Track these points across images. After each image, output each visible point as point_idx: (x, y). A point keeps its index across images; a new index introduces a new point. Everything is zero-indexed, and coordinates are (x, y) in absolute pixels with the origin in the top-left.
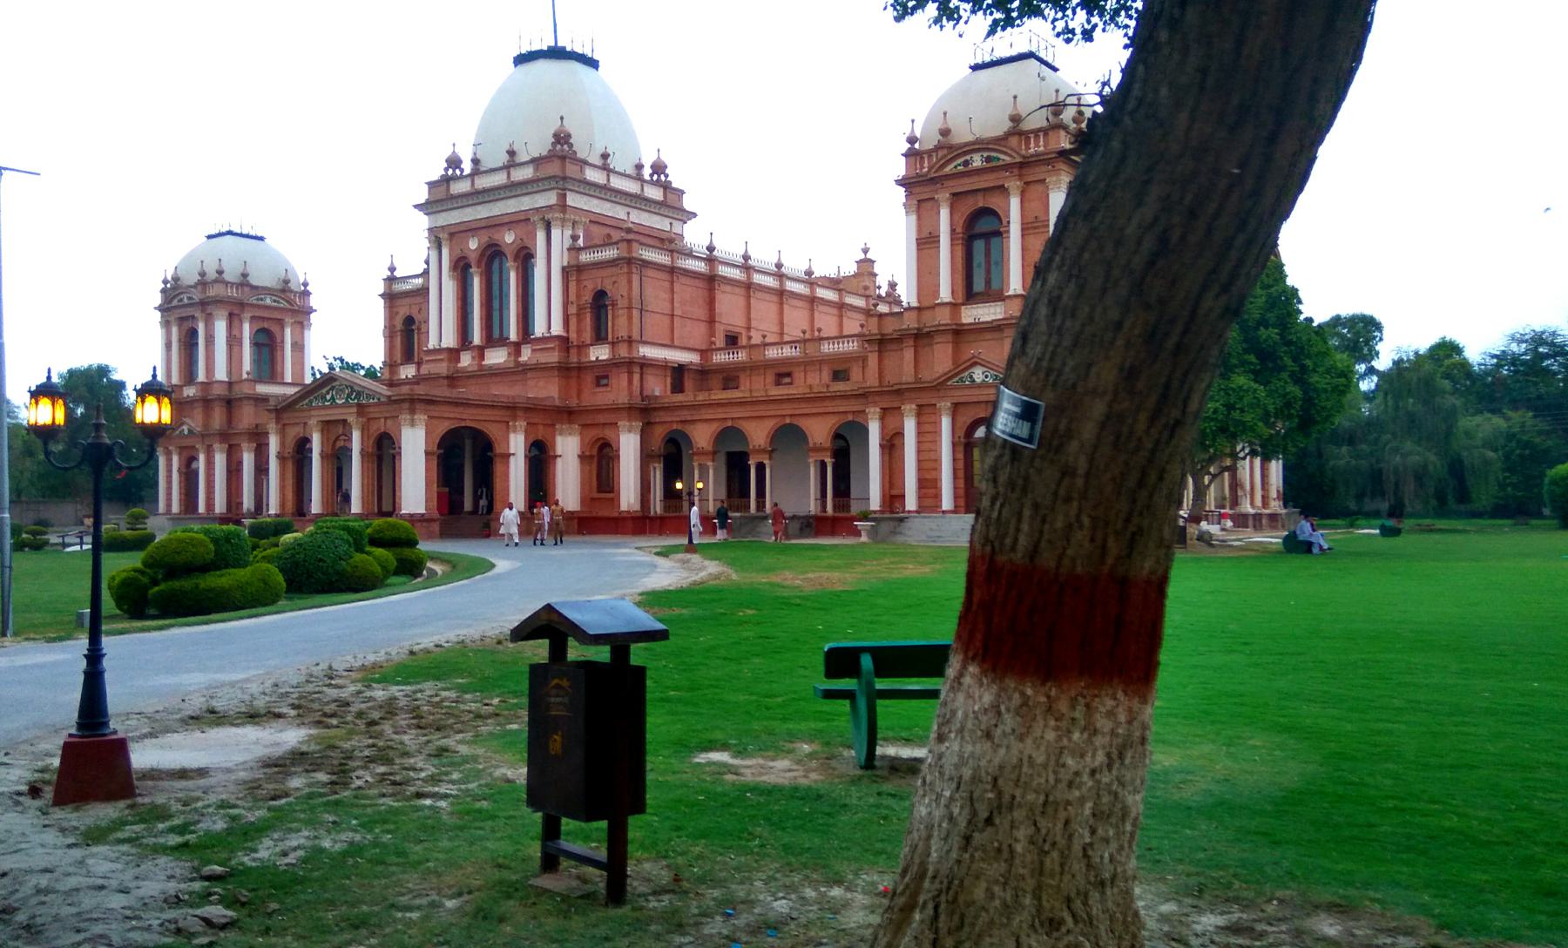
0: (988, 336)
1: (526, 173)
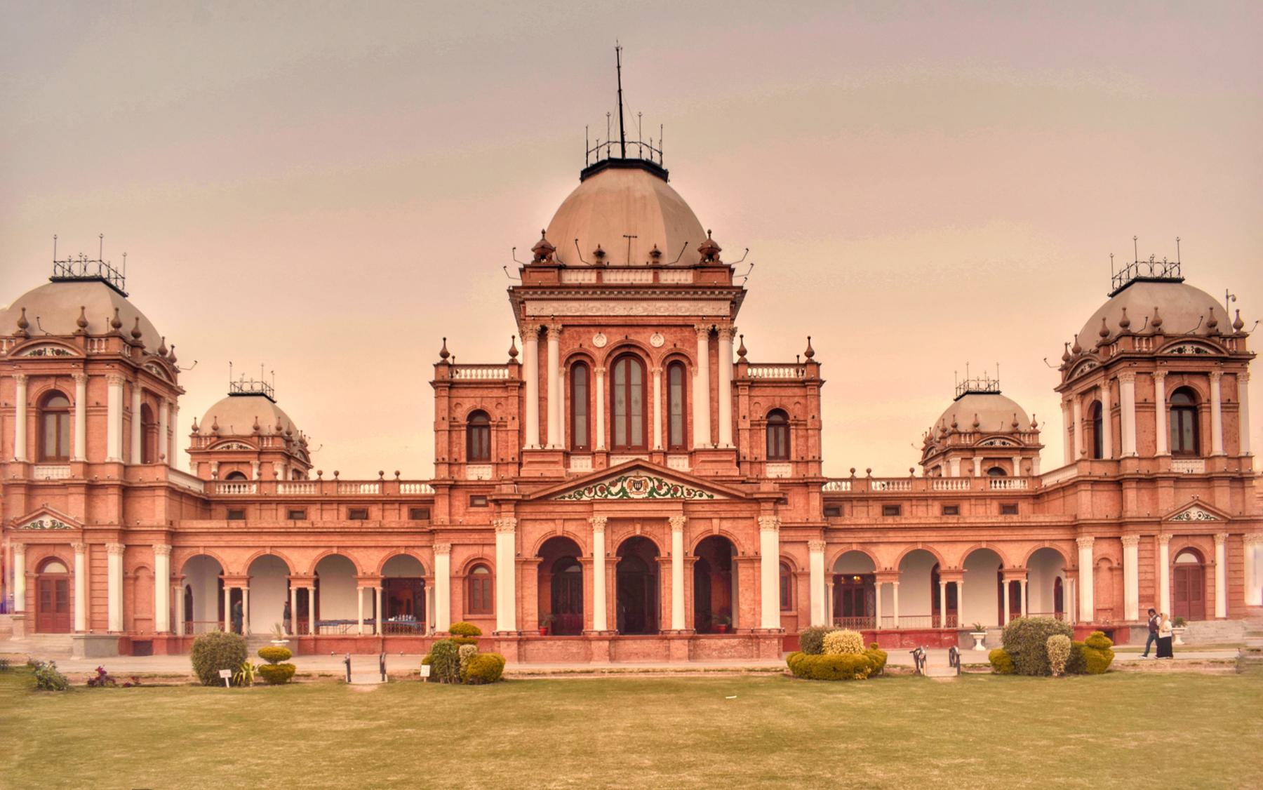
0: (1193, 485)
1: (686, 278)
